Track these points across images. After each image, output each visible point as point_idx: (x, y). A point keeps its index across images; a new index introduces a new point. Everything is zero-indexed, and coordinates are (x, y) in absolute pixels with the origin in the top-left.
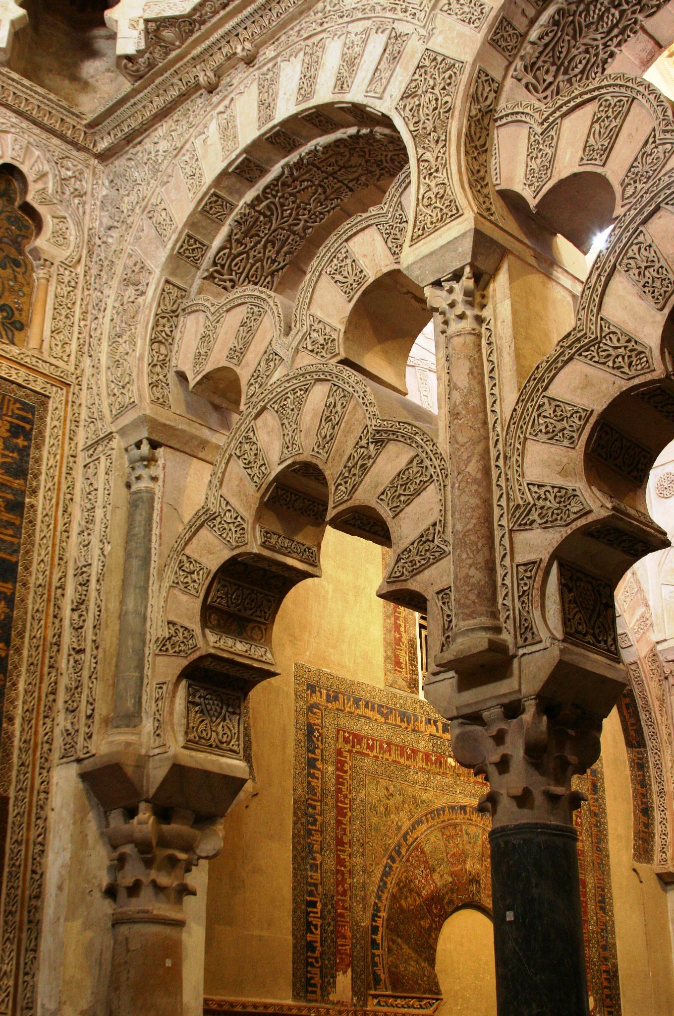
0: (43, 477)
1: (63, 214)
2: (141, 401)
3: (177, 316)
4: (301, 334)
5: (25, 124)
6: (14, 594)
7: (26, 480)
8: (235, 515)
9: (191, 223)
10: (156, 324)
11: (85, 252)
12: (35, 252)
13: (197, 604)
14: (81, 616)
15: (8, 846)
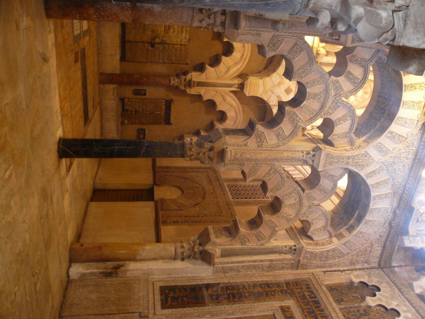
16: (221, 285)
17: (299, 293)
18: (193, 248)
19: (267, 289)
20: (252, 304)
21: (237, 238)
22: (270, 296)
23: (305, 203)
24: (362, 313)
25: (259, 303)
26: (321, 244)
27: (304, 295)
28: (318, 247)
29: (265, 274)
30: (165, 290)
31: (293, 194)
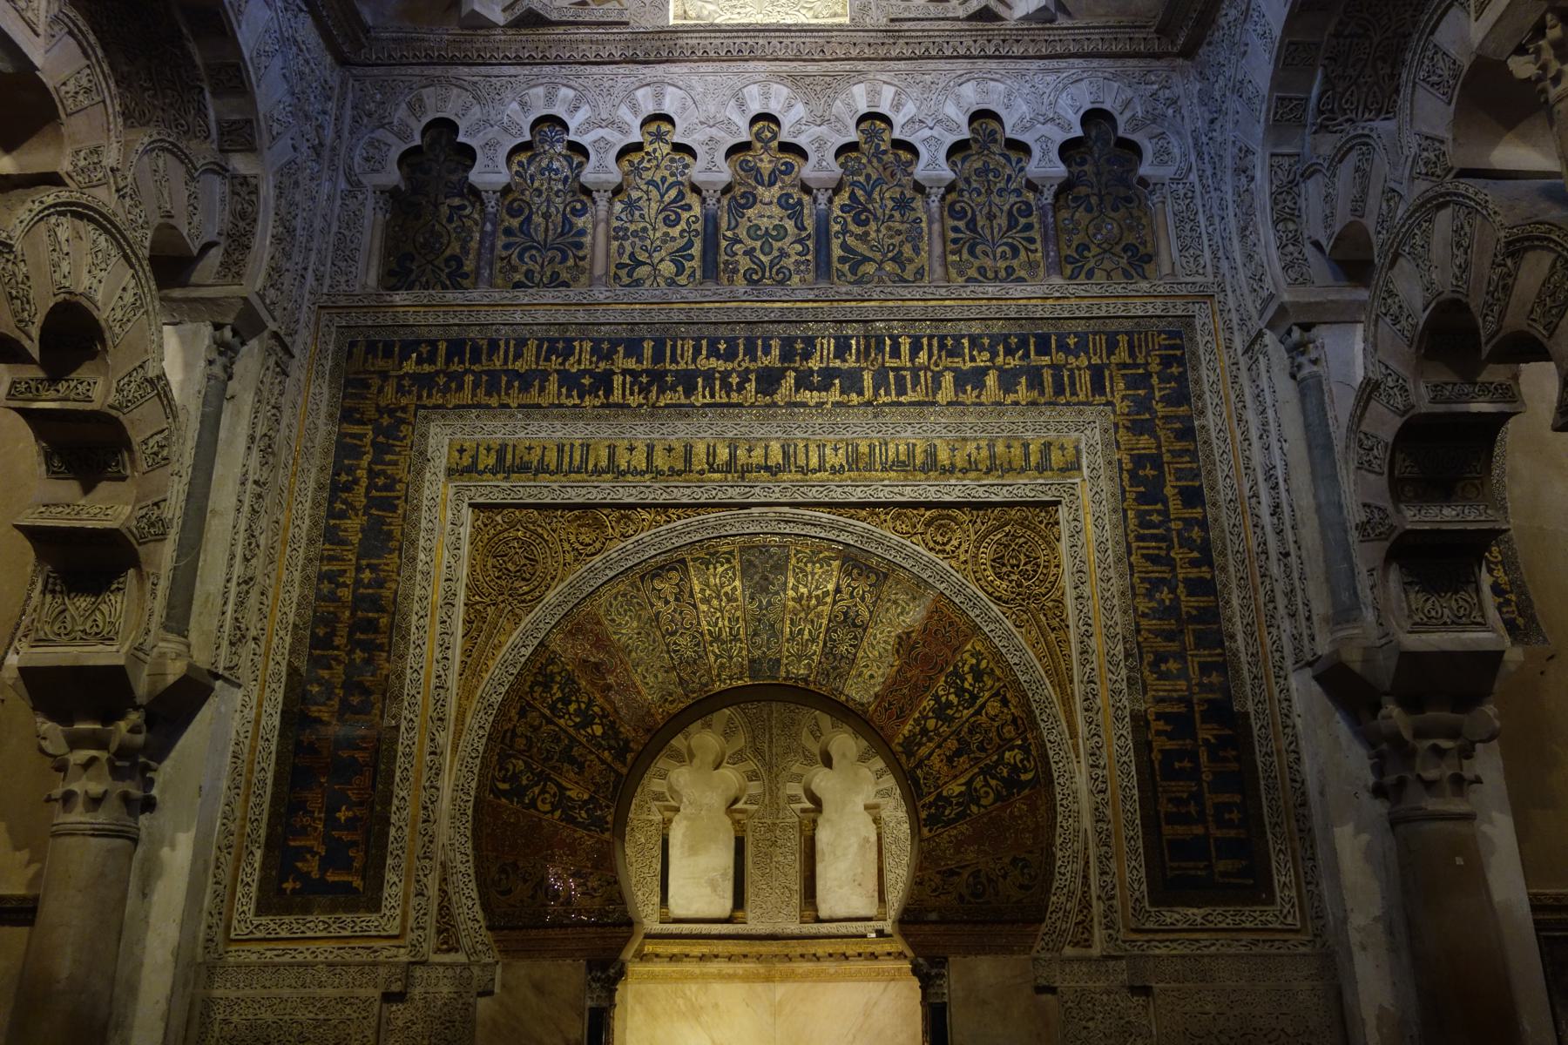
0: (1207, 396)
1: (1160, 130)
2: (1277, 289)
3: (1297, 185)
4: (1410, 159)
5: (1095, 63)
6: (1205, 516)
7: (1190, 405)
8: (1395, 377)
9: (1277, 82)
10: (1275, 202)
11: (1193, 158)
12: (1143, 182)
13: (1383, 481)
14: (1279, 519)
15: (1259, 760)
16: (302, 665)
17: (400, 389)
18: (124, 752)
19: (359, 496)
20: (420, 567)
21: (141, 550)
22: (392, 494)
23: (105, 197)
24: (522, 224)
25: (422, 542)
26: (241, 224)
27: (415, 377)
28: (256, 243)
29: (282, 478)
30: (282, 892)
31: (59, 231)
